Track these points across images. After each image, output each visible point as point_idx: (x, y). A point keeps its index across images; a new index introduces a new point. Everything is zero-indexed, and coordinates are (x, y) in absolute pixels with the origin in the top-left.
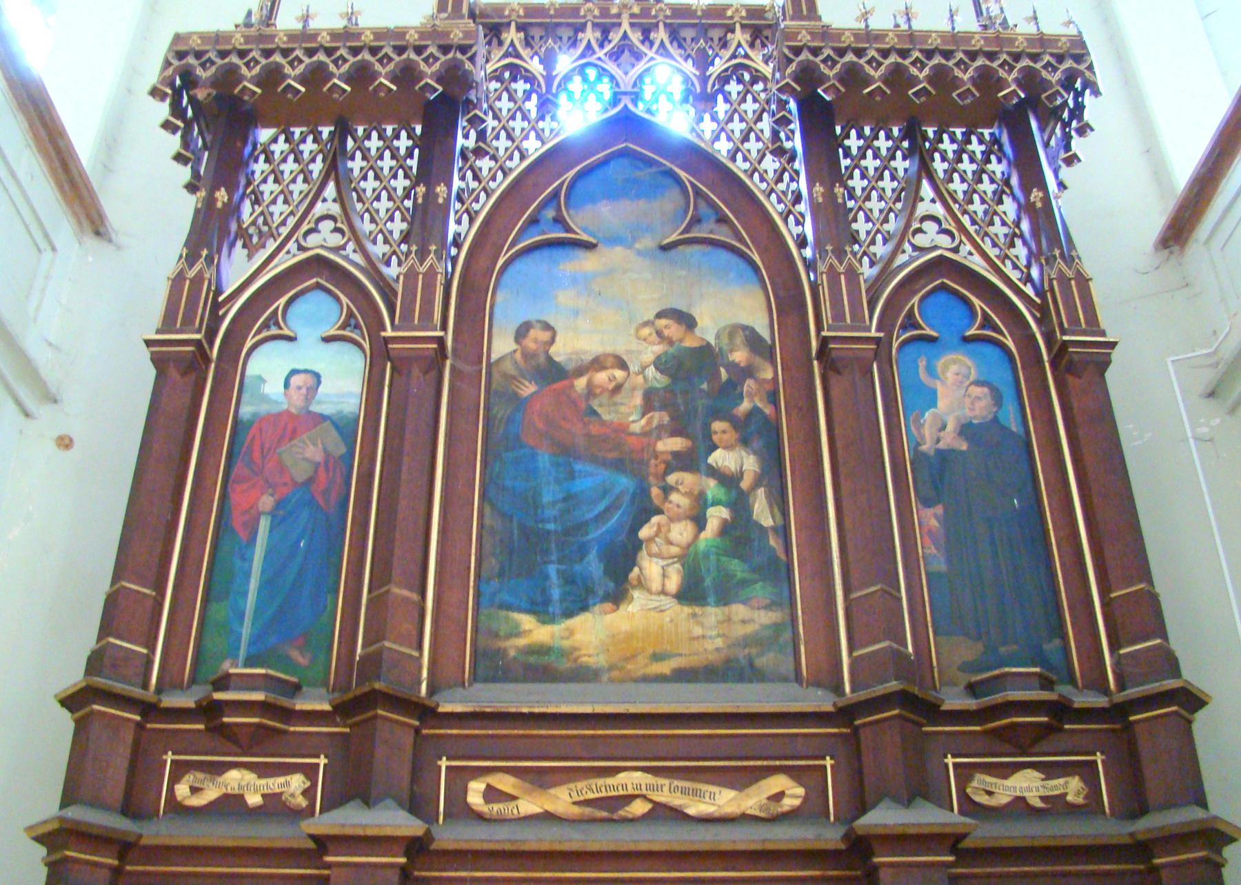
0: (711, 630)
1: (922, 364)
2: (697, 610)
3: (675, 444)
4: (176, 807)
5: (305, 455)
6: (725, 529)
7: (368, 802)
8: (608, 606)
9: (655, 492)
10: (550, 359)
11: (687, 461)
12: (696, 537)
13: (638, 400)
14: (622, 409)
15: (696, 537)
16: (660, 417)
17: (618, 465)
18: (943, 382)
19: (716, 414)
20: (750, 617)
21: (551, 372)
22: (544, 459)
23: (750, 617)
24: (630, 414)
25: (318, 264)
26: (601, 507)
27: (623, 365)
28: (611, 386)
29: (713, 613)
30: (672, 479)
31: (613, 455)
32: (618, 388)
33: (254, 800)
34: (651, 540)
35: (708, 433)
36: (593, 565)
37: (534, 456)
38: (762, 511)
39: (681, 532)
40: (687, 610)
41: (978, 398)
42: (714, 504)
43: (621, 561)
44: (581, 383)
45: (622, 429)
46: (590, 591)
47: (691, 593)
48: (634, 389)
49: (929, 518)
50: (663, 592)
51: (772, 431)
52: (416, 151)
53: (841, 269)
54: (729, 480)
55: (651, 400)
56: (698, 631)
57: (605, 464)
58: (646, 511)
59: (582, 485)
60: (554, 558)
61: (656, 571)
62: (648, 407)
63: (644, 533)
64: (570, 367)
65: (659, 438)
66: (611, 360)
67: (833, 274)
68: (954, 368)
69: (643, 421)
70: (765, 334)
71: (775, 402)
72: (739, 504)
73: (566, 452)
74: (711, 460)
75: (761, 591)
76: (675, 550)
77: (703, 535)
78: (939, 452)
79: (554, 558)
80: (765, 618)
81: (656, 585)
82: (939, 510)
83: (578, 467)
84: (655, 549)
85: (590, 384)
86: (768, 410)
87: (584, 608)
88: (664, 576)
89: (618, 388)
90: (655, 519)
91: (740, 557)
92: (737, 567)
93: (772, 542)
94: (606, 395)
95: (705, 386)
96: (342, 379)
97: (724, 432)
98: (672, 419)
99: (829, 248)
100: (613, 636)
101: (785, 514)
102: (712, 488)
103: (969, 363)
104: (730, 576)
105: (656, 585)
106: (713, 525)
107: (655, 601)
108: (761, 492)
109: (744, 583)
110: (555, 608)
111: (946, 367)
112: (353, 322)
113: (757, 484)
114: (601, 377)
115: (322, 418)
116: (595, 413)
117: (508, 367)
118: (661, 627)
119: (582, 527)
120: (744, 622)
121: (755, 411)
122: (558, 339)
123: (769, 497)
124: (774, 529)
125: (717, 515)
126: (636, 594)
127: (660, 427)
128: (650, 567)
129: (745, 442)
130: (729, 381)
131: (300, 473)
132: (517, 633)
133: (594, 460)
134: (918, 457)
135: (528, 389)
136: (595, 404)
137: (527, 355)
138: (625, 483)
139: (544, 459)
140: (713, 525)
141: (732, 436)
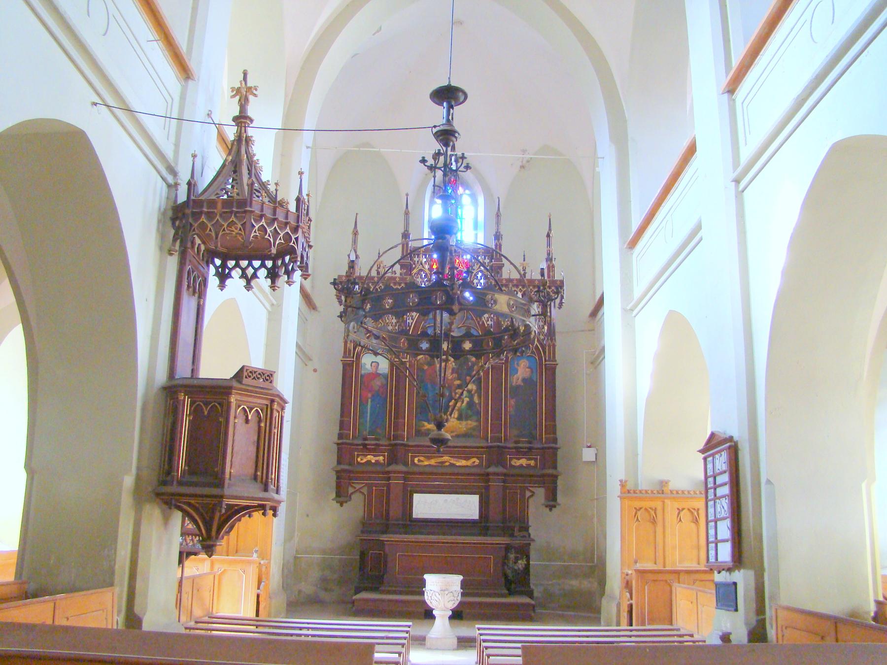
0: (463, 426)
3: (458, 382)
4: (359, 463)
5: (377, 383)
6: (468, 403)
7: (396, 463)
16: (455, 375)
19: (467, 375)
20: (472, 423)
22: (429, 386)
23: (472, 423)
29: (464, 423)
35: (466, 380)
54: (469, 391)
62: (452, 373)
72: (471, 397)
75: (475, 418)
80: (475, 424)
92: (469, 412)
96: (384, 365)
109: (470, 416)
115: (380, 375)
125: (466, 400)
131: (377, 388)
132: (424, 426)
134: (511, 385)
139: (429, 386)
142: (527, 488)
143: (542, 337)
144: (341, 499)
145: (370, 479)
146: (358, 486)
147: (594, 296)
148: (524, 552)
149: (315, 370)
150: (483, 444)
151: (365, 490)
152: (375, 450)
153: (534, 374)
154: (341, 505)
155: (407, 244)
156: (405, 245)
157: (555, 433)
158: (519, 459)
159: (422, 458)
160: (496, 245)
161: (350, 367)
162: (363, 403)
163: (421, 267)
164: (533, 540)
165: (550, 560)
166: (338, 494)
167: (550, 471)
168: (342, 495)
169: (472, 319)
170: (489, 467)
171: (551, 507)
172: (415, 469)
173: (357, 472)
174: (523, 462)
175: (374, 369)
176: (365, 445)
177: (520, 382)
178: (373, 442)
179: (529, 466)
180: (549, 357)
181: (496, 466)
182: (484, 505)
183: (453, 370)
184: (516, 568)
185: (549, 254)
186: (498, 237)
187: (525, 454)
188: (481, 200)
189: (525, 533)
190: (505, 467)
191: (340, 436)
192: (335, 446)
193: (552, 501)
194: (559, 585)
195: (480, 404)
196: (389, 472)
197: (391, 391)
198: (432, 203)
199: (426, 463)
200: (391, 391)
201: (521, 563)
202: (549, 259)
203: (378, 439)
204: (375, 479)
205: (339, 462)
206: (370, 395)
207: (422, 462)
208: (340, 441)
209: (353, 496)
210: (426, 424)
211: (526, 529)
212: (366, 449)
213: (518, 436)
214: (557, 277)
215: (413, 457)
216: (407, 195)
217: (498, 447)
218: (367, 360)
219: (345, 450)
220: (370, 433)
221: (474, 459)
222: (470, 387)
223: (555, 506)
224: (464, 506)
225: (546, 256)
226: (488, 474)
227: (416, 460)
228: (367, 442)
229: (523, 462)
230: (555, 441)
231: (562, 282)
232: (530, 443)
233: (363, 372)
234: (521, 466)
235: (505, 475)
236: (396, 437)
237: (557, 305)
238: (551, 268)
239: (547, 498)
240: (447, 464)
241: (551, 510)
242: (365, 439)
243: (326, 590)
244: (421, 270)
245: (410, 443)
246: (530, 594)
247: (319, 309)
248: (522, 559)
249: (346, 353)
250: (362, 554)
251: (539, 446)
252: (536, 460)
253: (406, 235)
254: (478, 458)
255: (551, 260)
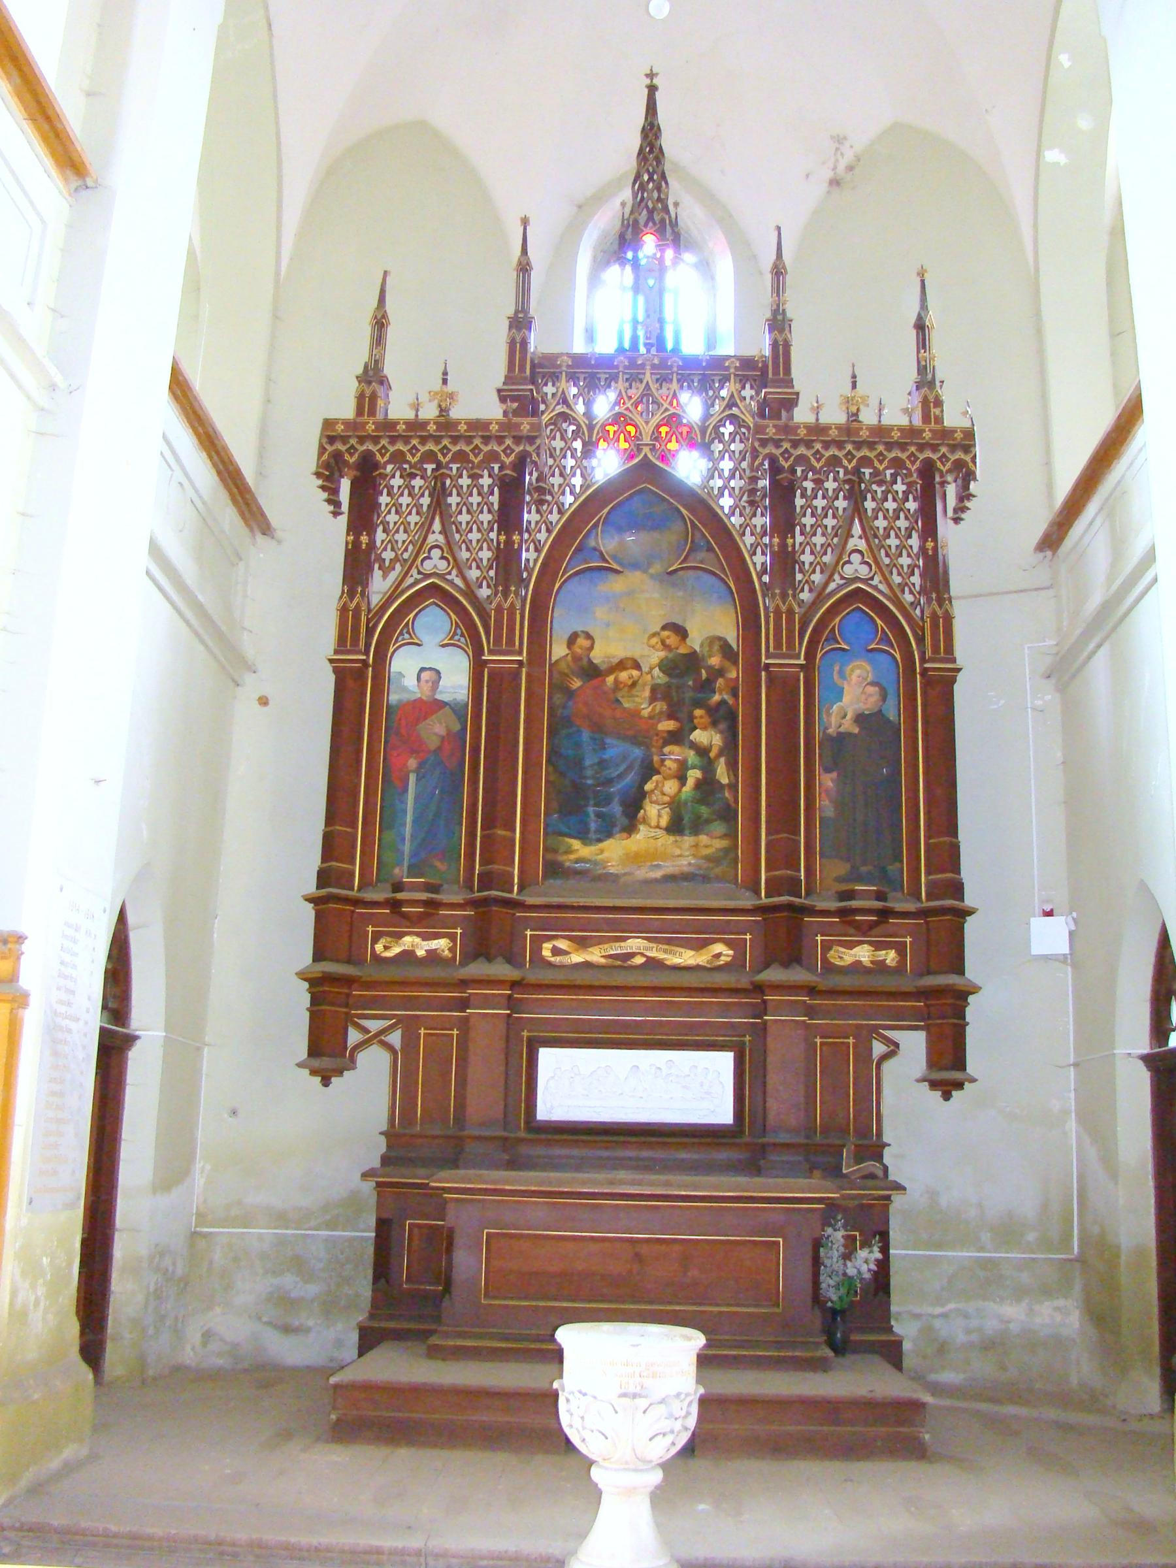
1: (836, 668)
2: (678, 838)
3: (668, 725)
6: (699, 785)
7: (489, 959)
8: (625, 835)
9: (656, 758)
10: (590, 662)
11: (676, 738)
12: (680, 791)
13: (647, 693)
14: (637, 699)
15: (680, 791)
16: (661, 706)
17: (635, 740)
18: (849, 683)
19: (698, 704)
21: (592, 672)
24: (642, 703)
25: (435, 592)
26: (622, 769)
27: (637, 666)
28: (630, 682)
29: (688, 840)
30: (667, 750)
31: (631, 733)
32: (634, 684)
33: (421, 953)
34: (652, 791)
35: (691, 718)
36: (616, 808)
37: (579, 732)
38: (722, 774)
39: (671, 787)
40: (672, 838)
41: (870, 695)
42: (693, 767)
43: (634, 805)
44: (610, 680)
45: (635, 714)
46: (614, 825)
47: (675, 827)
48: (645, 685)
49: (827, 781)
50: (658, 827)
51: (732, 717)
52: (496, 526)
53: (784, 608)
54: (702, 751)
55: (656, 693)
56: (678, 852)
57: (625, 738)
58: (649, 770)
59: (609, 754)
60: (592, 802)
61: (655, 812)
62: (653, 699)
63: (648, 787)
64: (603, 667)
65: (659, 721)
66: (630, 663)
67: (778, 613)
68: (858, 672)
69: (650, 709)
70: (735, 646)
71: (735, 694)
72: (708, 768)
73: (598, 728)
74: (692, 737)
75: (719, 828)
76: (667, 799)
77: (684, 789)
78: (839, 734)
79: (592, 802)
81: (653, 823)
82: (834, 775)
83: (608, 741)
84: (654, 798)
85: (616, 680)
86: (731, 701)
87: (609, 835)
88: (659, 816)
89: (634, 684)
90: (654, 778)
91: (708, 804)
92: (704, 810)
93: (727, 794)
94: (626, 689)
95: (690, 683)
97: (701, 717)
98: (669, 706)
99: (777, 591)
100: (627, 854)
101: (736, 776)
102: (692, 757)
103: (869, 668)
104: (699, 817)
105: (653, 823)
106: (690, 782)
107: (653, 833)
108: (722, 760)
109: (708, 822)
110: (592, 836)
111: (852, 671)
112: (459, 631)
113: (719, 755)
114: (624, 676)
116: (618, 701)
117: (563, 666)
118: (656, 849)
119: (609, 782)
120: (706, 846)
121: (723, 702)
122: (596, 646)
123: (728, 764)
124: (728, 785)
125: (694, 775)
126: (641, 827)
127: (661, 712)
128: (651, 810)
129: (714, 724)
130: (707, 679)
132: (569, 851)
133: (619, 736)
135: (576, 684)
136: (619, 695)
137: (577, 659)
138: (637, 752)
140: (690, 782)
141: (706, 720)
142: (875, 1028)
143: (908, 598)
144: (324, 1062)
145: (408, 1003)
146: (374, 1025)
147: (1050, 486)
148: (872, 1225)
149: (264, 701)
150: (747, 902)
151: (395, 1038)
152: (428, 918)
153: (891, 702)
154: (326, 1082)
155: (524, 343)
156: (517, 348)
157: (956, 867)
158: (851, 945)
159: (563, 944)
160: (775, 345)
161: (356, 684)
162: (394, 783)
163: (560, 409)
164: (900, 1188)
165: (939, 1246)
166: (315, 1050)
167: (952, 979)
168: (327, 1052)
169: (710, 549)
170: (767, 966)
171: (947, 1089)
172: (547, 977)
173: (370, 985)
174: (863, 954)
175: (426, 688)
176: (395, 905)
177: (849, 726)
178: (424, 896)
179: (880, 967)
180: (936, 649)
181: (786, 965)
182: (748, 1084)
183: (654, 690)
184: (851, 1271)
185: (922, 369)
186: (779, 323)
187: (865, 930)
188: (725, 266)
189: (870, 1166)
190: (812, 969)
191: (323, 878)
192: (309, 911)
193: (948, 1068)
194: (966, 1316)
195: (733, 787)
196: (464, 983)
197: (475, 750)
198: (594, 279)
199: (577, 958)
200: (475, 750)
201: (865, 1260)
202: (926, 380)
203: (434, 888)
204: (429, 1004)
205: (319, 955)
206: (412, 763)
207: (565, 953)
208: (323, 892)
209: (362, 1057)
210: (576, 844)
211: (874, 1150)
212: (398, 915)
213: (839, 880)
214: (952, 418)
215: (538, 942)
216: (525, 222)
217: (790, 907)
218: (405, 666)
219: (338, 915)
220: (414, 870)
221: (719, 948)
222: (700, 736)
223: (959, 1085)
224: (692, 1086)
225: (913, 375)
226: (759, 989)
227: (546, 952)
228: (400, 896)
229: (863, 954)
230: (957, 889)
231: (969, 434)
232: (880, 896)
233: (394, 698)
234: (857, 966)
235: (812, 991)
236: (487, 881)
237: (950, 513)
238: (931, 404)
239: (934, 1061)
240: (639, 960)
241: (947, 1096)
242: (398, 887)
243: (287, 1329)
244: (564, 417)
245: (531, 901)
246: (892, 1353)
247: (279, 534)
248: (866, 1244)
249: (347, 636)
250: (384, 1227)
251: (911, 907)
252: (900, 949)
253: (520, 322)
254: (729, 943)
255: (931, 384)
